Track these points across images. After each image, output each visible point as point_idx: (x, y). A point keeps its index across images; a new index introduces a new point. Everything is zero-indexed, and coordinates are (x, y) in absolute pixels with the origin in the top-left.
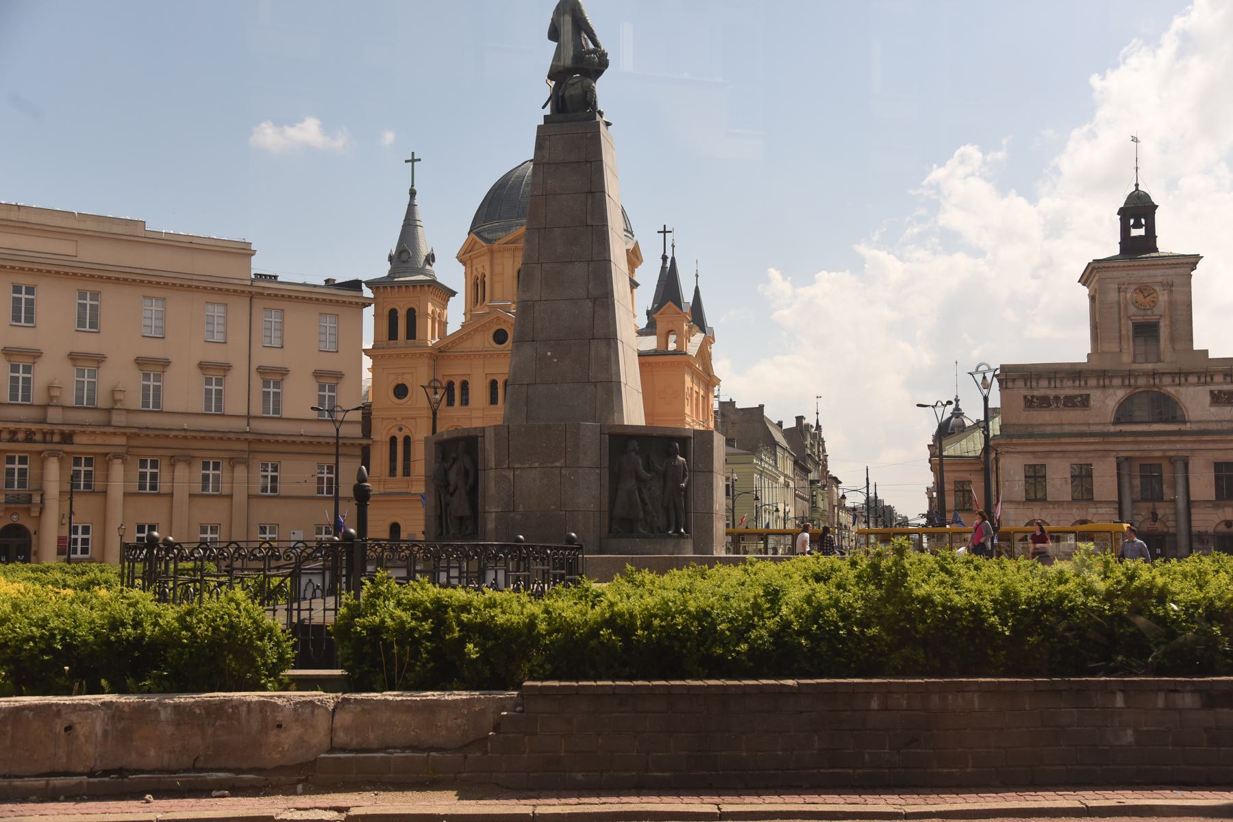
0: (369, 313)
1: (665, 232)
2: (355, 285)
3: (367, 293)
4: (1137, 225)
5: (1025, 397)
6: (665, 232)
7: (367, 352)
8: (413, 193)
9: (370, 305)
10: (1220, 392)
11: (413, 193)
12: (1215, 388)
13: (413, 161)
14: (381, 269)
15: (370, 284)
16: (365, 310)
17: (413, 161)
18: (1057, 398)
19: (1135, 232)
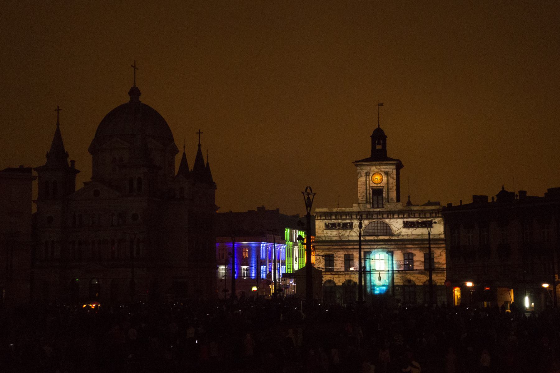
0: (35, 183)
1: (199, 133)
2: (29, 170)
3: (35, 173)
4: (379, 144)
5: (326, 223)
6: (199, 133)
7: (34, 201)
8: (58, 124)
9: (35, 179)
10: (407, 222)
11: (58, 124)
12: (405, 220)
13: (58, 110)
14: (42, 162)
15: (36, 169)
16: (33, 182)
17: (58, 110)
18: (339, 224)
19: (379, 147)
